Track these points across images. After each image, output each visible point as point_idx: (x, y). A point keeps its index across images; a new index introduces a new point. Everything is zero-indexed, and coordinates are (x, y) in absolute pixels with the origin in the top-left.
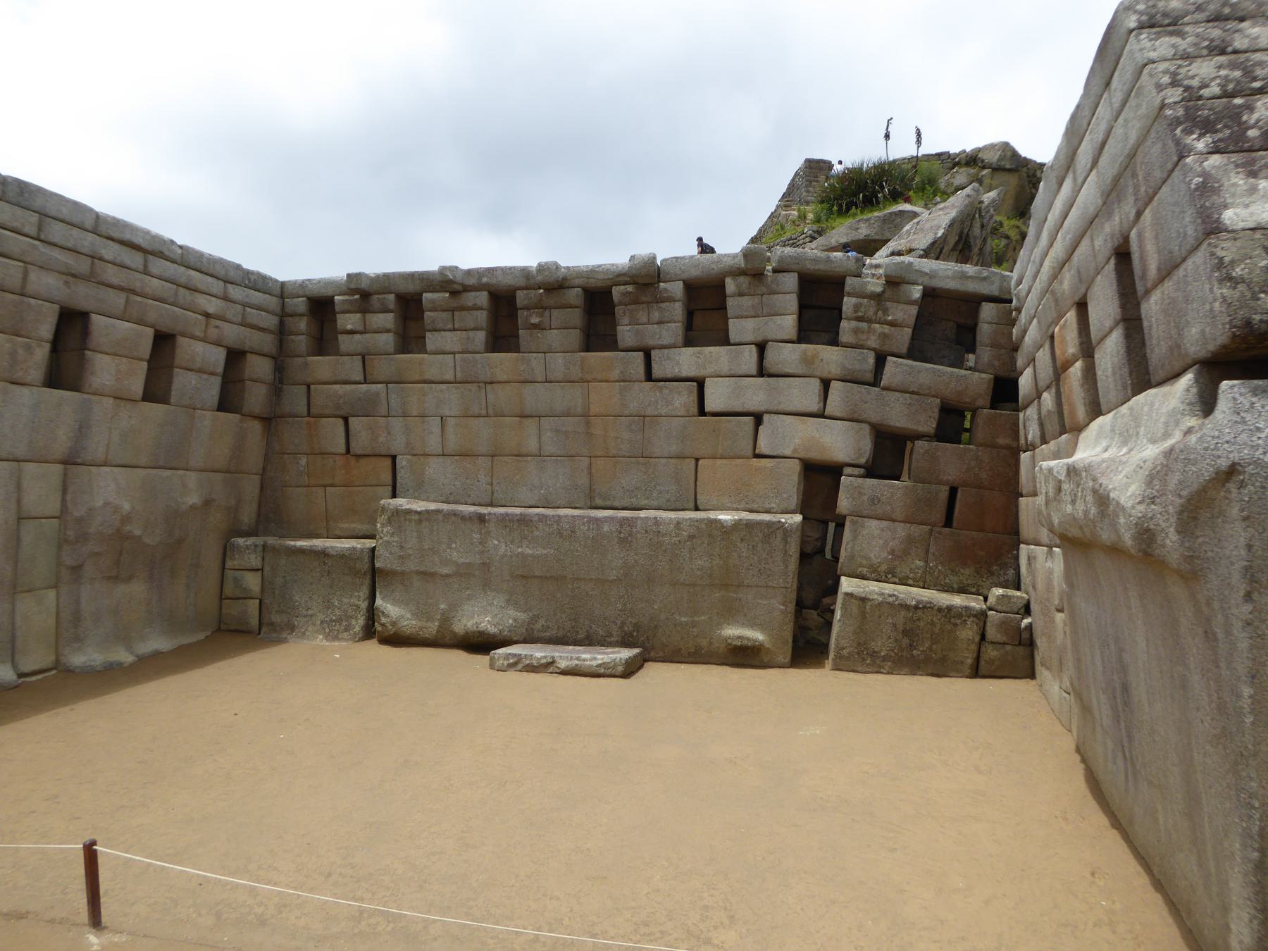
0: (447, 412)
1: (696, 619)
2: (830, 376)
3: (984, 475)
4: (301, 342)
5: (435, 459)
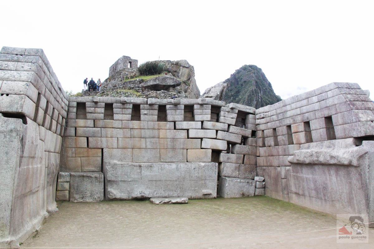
0: (119, 136)
1: (195, 188)
2: (218, 129)
3: (250, 152)
4: (73, 115)
5: (115, 149)
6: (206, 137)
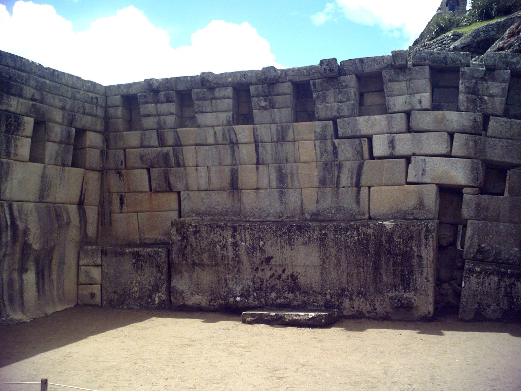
2: (455, 130)
4: (120, 123)
6: (417, 152)
